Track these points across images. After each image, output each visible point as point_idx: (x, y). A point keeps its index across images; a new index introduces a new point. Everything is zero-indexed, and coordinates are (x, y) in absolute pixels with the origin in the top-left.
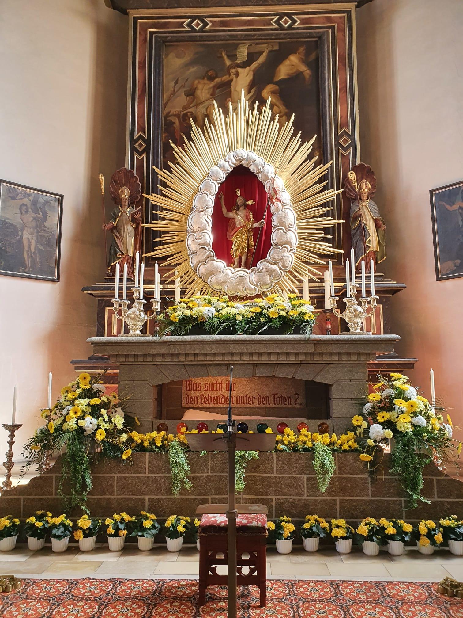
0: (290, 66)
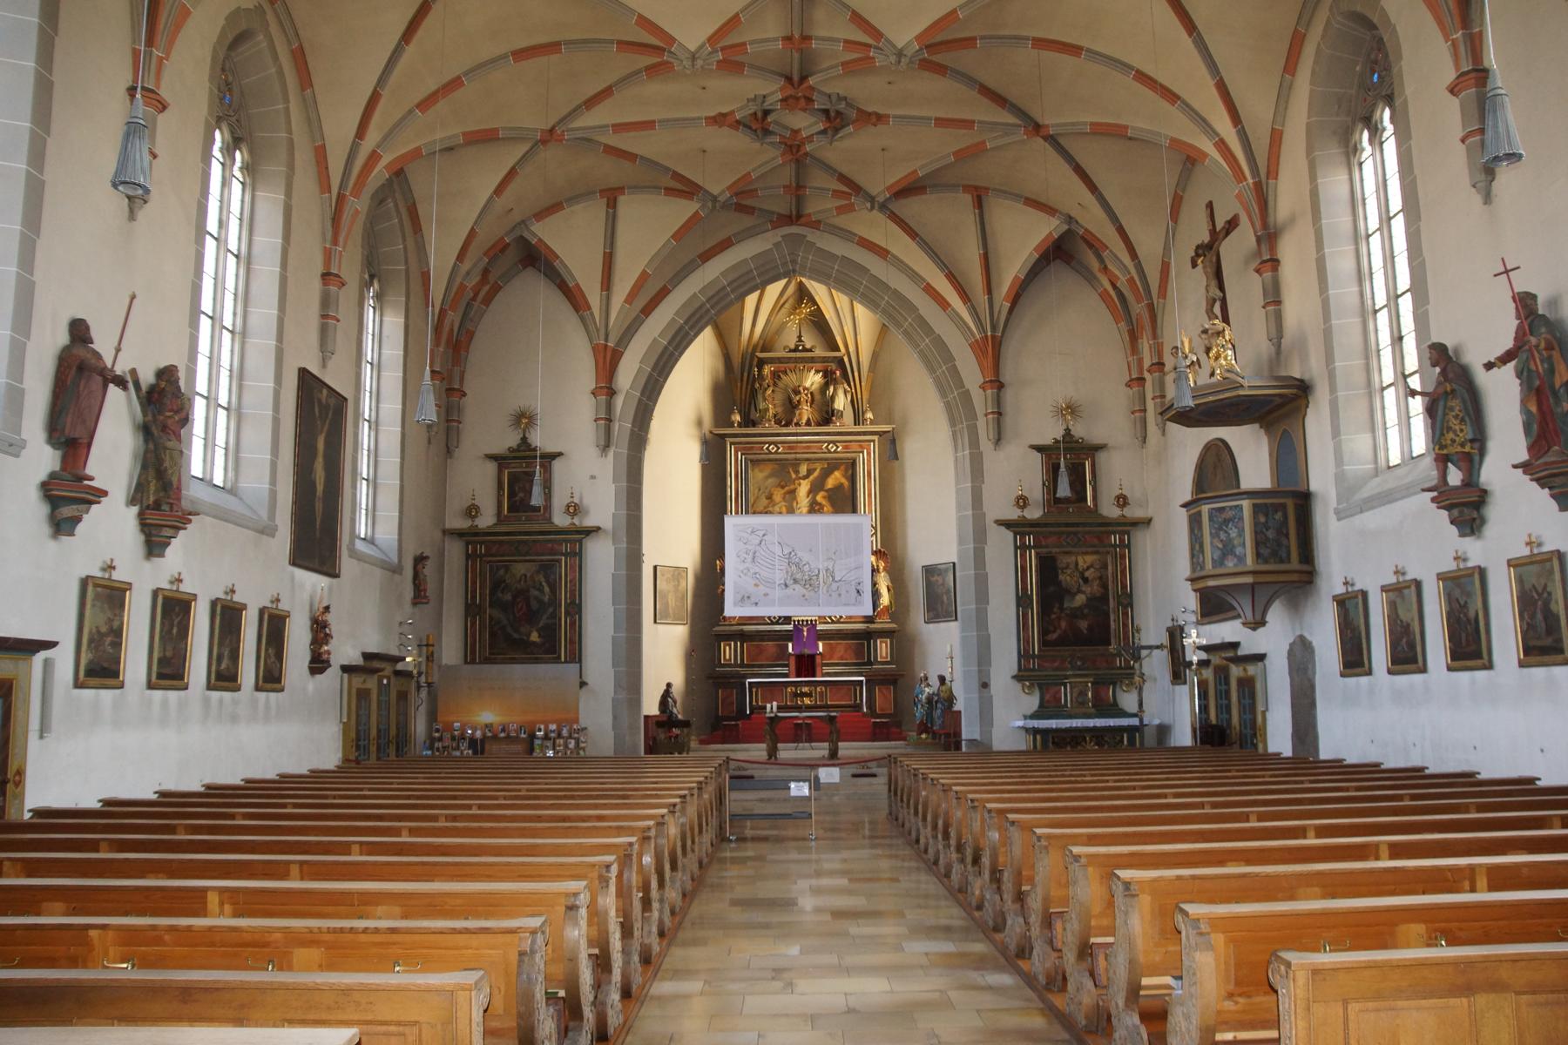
0: (836, 479)
